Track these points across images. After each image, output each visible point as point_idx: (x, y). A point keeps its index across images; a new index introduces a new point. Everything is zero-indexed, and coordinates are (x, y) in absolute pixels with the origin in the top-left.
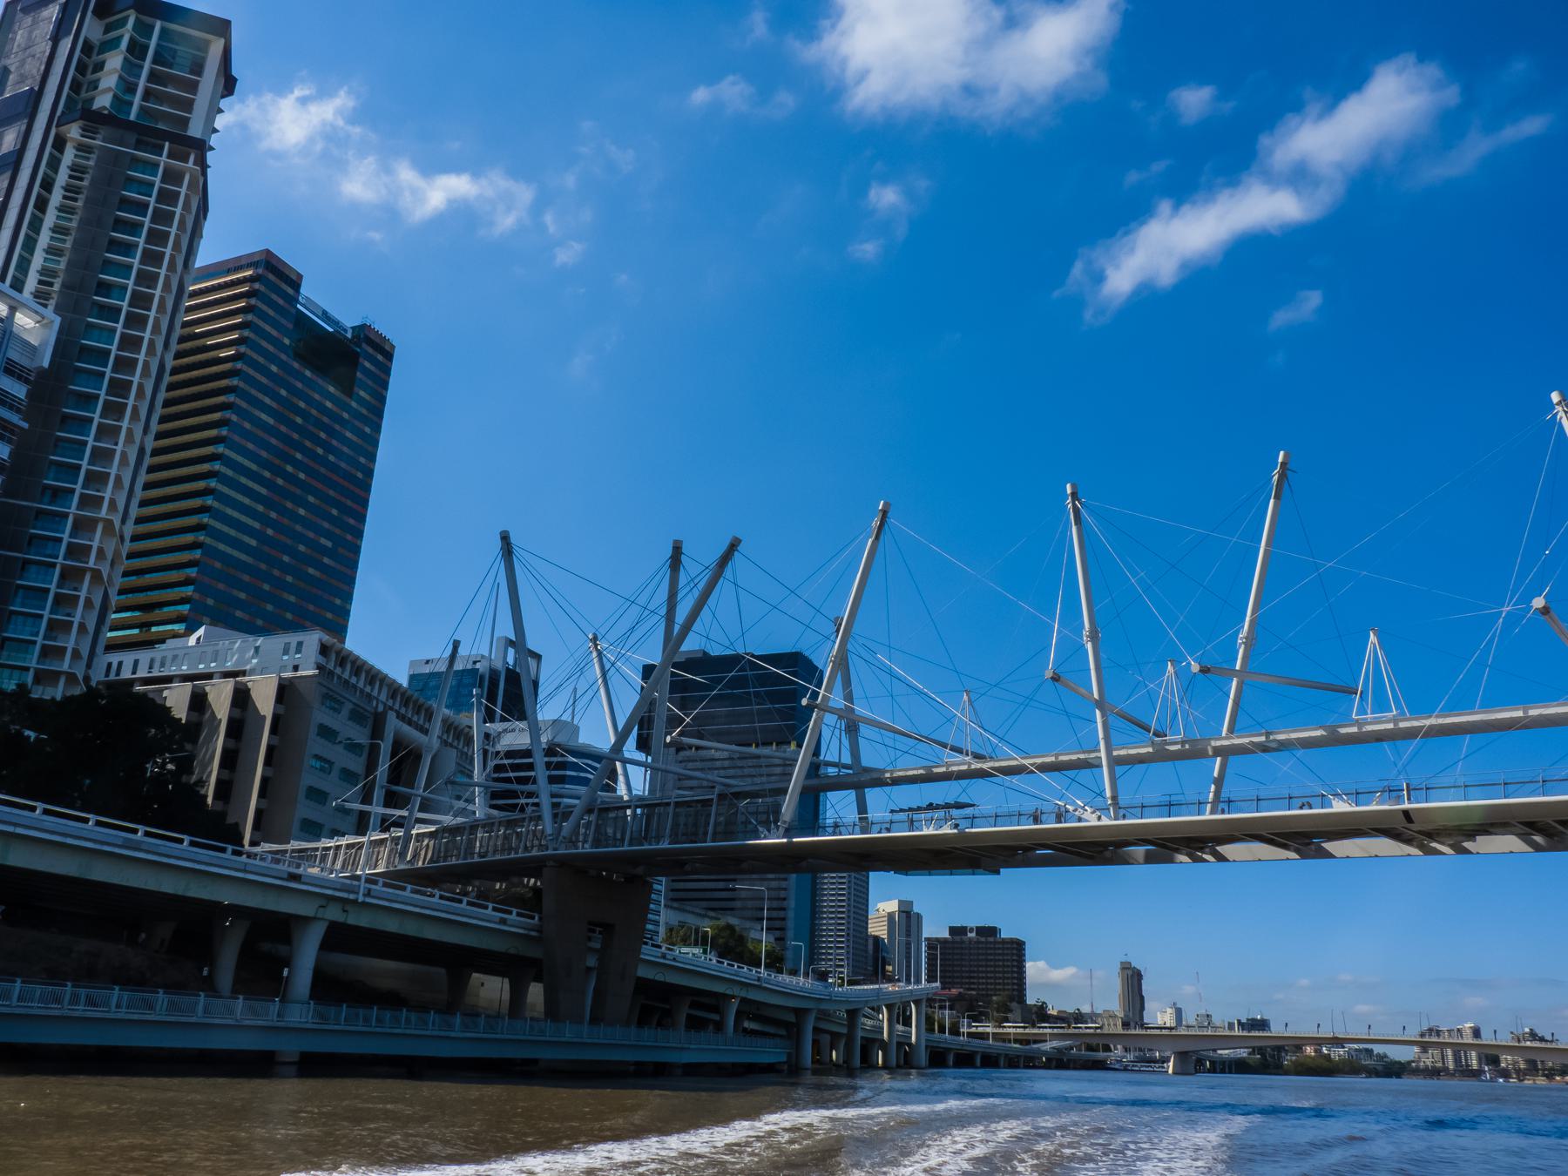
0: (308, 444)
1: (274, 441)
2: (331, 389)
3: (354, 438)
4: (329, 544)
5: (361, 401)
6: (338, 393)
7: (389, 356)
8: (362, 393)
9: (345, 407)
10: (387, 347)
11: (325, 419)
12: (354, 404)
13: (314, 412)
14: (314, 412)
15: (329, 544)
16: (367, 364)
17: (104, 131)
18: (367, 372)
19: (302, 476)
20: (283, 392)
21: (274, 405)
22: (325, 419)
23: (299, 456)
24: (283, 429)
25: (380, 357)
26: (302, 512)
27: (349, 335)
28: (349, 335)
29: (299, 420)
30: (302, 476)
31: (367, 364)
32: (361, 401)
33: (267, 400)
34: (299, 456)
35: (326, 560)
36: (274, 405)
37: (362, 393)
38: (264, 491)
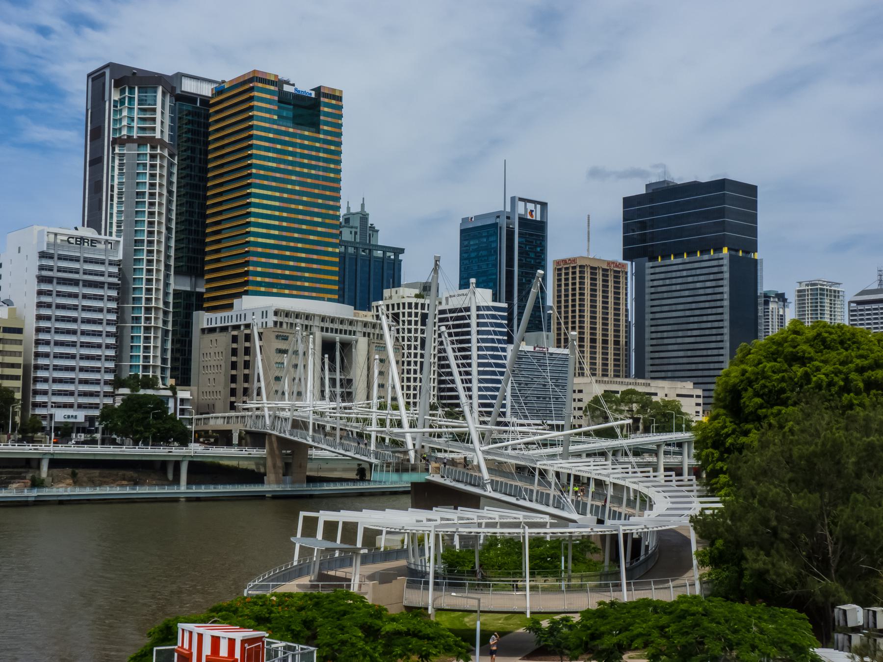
0: (298, 169)
1: (278, 175)
2: (306, 133)
4: (320, 220)
5: (327, 133)
6: (311, 134)
7: (339, 99)
8: (326, 128)
9: (318, 140)
10: (337, 94)
11: (306, 152)
12: (321, 136)
13: (298, 150)
14: (298, 150)
15: (320, 220)
16: (326, 109)
18: (327, 114)
19: (297, 188)
22: (306, 152)
23: (294, 178)
24: (282, 166)
25: (334, 102)
26: (301, 207)
27: (313, 96)
28: (313, 96)
29: (290, 158)
30: (297, 188)
31: (326, 109)
32: (327, 133)
33: (270, 155)
34: (294, 178)
35: (319, 229)
37: (326, 128)
38: (277, 204)
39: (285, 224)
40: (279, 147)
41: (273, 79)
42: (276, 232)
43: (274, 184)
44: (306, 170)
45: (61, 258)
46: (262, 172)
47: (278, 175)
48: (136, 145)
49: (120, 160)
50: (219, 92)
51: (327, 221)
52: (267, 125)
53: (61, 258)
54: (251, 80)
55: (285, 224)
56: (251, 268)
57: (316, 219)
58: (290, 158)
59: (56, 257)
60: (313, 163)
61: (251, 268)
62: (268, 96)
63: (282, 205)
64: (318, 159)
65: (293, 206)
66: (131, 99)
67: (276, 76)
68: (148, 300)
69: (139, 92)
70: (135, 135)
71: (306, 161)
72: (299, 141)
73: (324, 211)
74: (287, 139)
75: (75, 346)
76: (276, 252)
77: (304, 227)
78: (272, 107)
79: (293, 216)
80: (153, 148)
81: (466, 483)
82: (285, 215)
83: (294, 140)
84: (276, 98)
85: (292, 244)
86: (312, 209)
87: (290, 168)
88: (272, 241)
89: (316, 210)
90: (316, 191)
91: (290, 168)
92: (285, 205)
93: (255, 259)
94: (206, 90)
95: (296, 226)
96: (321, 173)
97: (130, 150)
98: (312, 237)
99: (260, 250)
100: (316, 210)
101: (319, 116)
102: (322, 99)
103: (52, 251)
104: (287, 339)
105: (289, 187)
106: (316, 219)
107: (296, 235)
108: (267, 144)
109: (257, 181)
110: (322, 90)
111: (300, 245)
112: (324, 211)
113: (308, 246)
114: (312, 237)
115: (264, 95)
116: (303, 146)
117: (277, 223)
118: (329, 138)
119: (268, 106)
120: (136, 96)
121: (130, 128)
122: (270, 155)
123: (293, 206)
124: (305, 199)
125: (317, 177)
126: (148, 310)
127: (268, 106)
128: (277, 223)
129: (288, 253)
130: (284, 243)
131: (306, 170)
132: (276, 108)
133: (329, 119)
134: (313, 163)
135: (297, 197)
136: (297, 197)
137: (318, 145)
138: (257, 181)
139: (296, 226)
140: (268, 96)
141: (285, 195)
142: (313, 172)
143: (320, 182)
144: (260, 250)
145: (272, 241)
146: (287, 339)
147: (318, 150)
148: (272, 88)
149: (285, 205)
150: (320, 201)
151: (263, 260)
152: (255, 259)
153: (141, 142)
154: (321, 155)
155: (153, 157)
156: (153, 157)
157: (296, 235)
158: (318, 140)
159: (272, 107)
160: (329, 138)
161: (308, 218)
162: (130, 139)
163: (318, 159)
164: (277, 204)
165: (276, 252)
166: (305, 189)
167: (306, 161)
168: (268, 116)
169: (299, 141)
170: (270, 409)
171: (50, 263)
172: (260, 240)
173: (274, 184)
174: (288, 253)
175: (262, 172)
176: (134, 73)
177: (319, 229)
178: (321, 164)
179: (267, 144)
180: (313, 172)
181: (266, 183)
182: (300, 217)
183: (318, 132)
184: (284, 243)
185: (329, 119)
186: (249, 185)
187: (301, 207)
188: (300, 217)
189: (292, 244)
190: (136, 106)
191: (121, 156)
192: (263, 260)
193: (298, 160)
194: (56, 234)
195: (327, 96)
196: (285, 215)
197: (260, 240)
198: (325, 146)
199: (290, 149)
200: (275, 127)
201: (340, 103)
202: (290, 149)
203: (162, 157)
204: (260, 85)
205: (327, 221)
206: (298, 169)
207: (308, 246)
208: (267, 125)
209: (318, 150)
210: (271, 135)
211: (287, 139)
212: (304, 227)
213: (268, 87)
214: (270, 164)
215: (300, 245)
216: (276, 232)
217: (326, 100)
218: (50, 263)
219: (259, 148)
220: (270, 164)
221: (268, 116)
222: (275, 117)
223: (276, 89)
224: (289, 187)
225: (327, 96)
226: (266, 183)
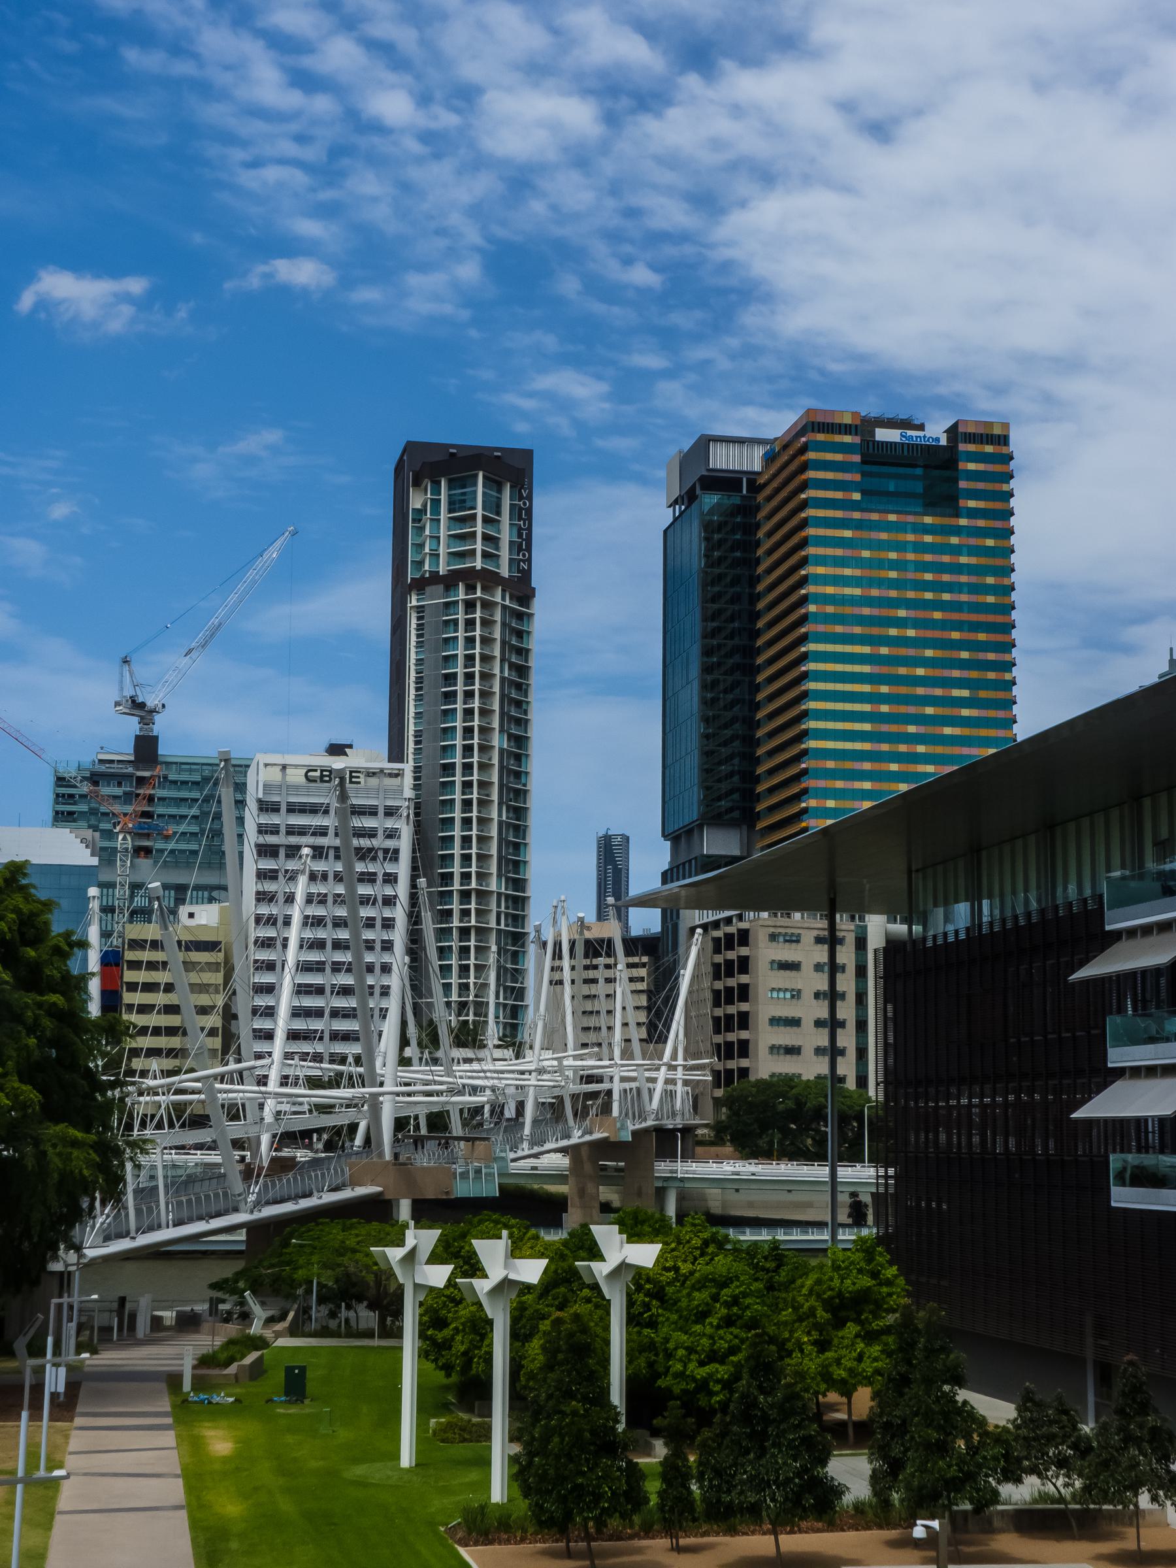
1: (866, 611)
2: (928, 520)
3: (973, 560)
4: (965, 693)
5: (973, 514)
6: (938, 520)
7: (1004, 440)
8: (972, 504)
10: (997, 431)
11: (928, 558)
12: (963, 522)
13: (911, 556)
14: (911, 556)
15: (965, 693)
16: (972, 466)
17: (429, 590)
19: (911, 633)
20: (866, 554)
21: (858, 572)
22: (928, 558)
23: (902, 613)
24: (875, 592)
25: (989, 449)
26: (920, 672)
27: (943, 442)
28: (943, 442)
29: (893, 574)
30: (911, 633)
31: (972, 466)
32: (973, 514)
33: (848, 572)
34: (902, 613)
35: (965, 712)
36: (858, 572)
37: (972, 504)
38: (866, 669)
39: (885, 708)
40: (866, 554)
41: (847, 420)
42: (867, 727)
43: (857, 630)
44: (929, 596)
45: (292, 809)
46: (830, 609)
47: (866, 611)
48: (441, 587)
49: (419, 618)
50: (769, 459)
51: (983, 694)
52: (839, 514)
53: (292, 809)
54: (802, 432)
55: (885, 708)
56: (813, 803)
57: (956, 693)
58: (893, 574)
59: (284, 808)
60: (946, 578)
61: (813, 803)
62: (839, 457)
63: (877, 669)
64: (958, 569)
65: (902, 671)
66: (436, 503)
67: (855, 414)
68: (466, 877)
69: (450, 488)
70: (442, 571)
71: (928, 577)
72: (910, 537)
73: (974, 674)
74: (884, 536)
75: (323, 970)
76: (867, 766)
77: (929, 710)
78: (848, 477)
79: (903, 690)
80: (471, 588)
81: (200, 1218)
82: (884, 689)
83: (901, 537)
84: (857, 458)
85: (903, 748)
86: (946, 673)
87: (893, 594)
88: (858, 746)
89: (956, 673)
90: (955, 635)
91: (893, 594)
92: (885, 670)
93: (822, 783)
94: (753, 461)
95: (912, 710)
96: (964, 598)
97: (434, 598)
98: (948, 731)
99: (830, 764)
100: (956, 673)
101: (956, 481)
102: (962, 447)
103: (276, 799)
104: (798, 941)
105: (893, 632)
106: (956, 693)
107: (912, 729)
108: (839, 552)
109: (821, 628)
110: (961, 429)
111: (921, 749)
112: (974, 674)
113: (939, 750)
114: (948, 731)
115: (829, 456)
116: (920, 547)
117: (867, 708)
118: (981, 523)
119: (839, 476)
120: (443, 497)
121: (435, 556)
122: (848, 572)
123: (902, 671)
124: (929, 653)
125: (956, 606)
126: (465, 895)
127: (839, 476)
128: (867, 708)
129: (894, 767)
130: (885, 747)
131: (929, 596)
132: (857, 477)
133: (980, 486)
134: (946, 578)
135: (911, 652)
136: (911, 652)
137: (954, 540)
138: (821, 628)
139: (912, 710)
140: (839, 457)
141: (884, 651)
142: (946, 597)
143: (965, 617)
144: (830, 764)
145: (858, 746)
146: (798, 941)
147: (956, 550)
148: (848, 439)
149: (885, 670)
150: (965, 655)
151: (839, 784)
152: (822, 783)
153: (449, 581)
154: (964, 560)
155: (470, 606)
156: (470, 606)
157: (912, 729)
158: (958, 531)
159: (848, 477)
160: (981, 523)
161: (938, 692)
162: (435, 578)
163: (958, 569)
164: (866, 669)
165: (867, 766)
166: (929, 634)
167: (928, 577)
168: (839, 495)
169: (910, 537)
170: (623, 1079)
171: (275, 819)
172: (830, 745)
173: (857, 630)
174: (894, 767)
175: (830, 609)
176: (453, 455)
177: (965, 712)
178: (964, 579)
179: (839, 552)
180: (946, 597)
181: (839, 629)
182: (920, 691)
183: (957, 515)
184: (885, 747)
185: (980, 486)
186: (804, 639)
187: (920, 672)
188: (920, 691)
189: (903, 748)
190: (444, 515)
191: (420, 609)
192: (839, 784)
193: (910, 575)
194: (284, 767)
195: (971, 438)
196: (884, 689)
197: (830, 745)
198: (973, 541)
199: (893, 555)
200: (857, 515)
201: (1004, 450)
202: (893, 555)
203: (487, 605)
204: (821, 437)
205: (983, 694)
206: (911, 595)
207: (939, 750)
208: (839, 514)
209: (956, 550)
210: (848, 534)
211: (884, 536)
212: (929, 710)
213: (838, 438)
214: (848, 591)
215: (921, 749)
216: (867, 727)
217: (971, 447)
218: (275, 819)
219: (822, 561)
220: (848, 591)
221: (839, 495)
222: (857, 496)
223: (857, 440)
224: (893, 632)
225: (971, 438)
226: (839, 629)
